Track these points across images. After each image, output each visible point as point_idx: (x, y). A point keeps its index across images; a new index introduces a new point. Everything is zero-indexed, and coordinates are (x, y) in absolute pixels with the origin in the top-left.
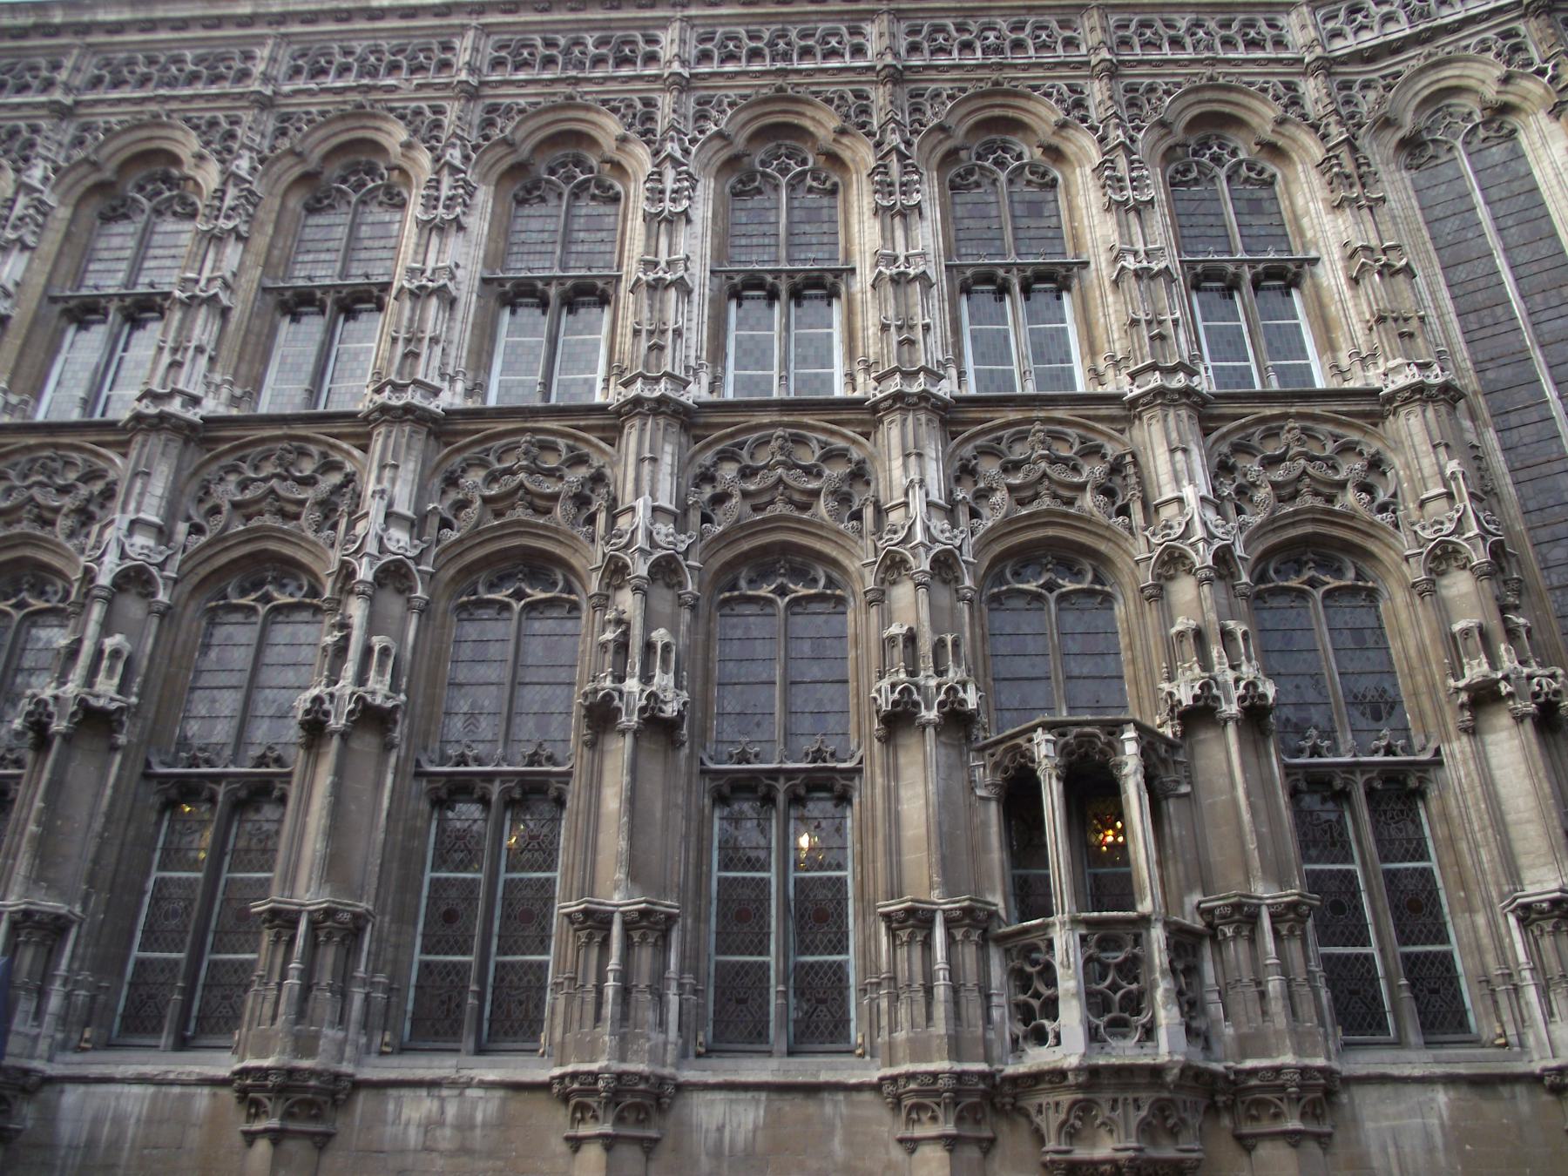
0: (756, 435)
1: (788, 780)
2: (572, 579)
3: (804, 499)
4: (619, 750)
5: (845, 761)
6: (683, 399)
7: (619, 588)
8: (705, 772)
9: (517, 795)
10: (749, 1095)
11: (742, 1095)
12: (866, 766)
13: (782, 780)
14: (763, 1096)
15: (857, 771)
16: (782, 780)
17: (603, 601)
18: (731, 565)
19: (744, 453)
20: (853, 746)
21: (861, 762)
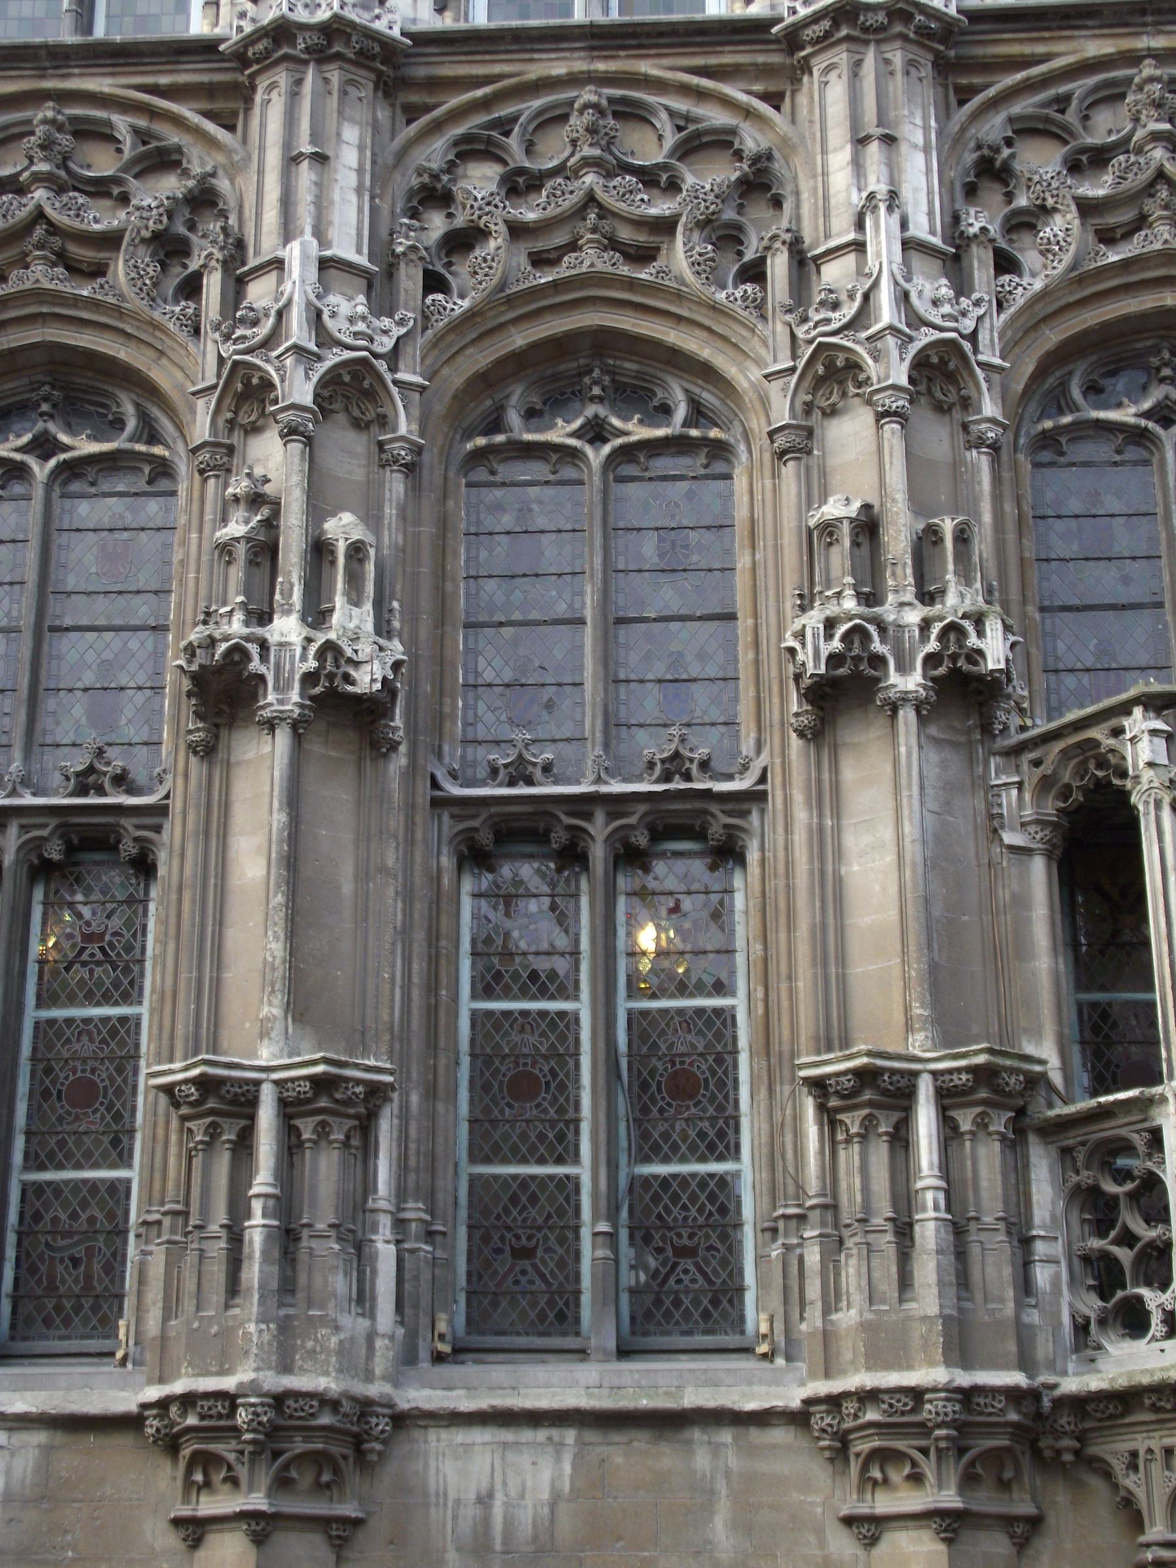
0: (537, 103)
1: (612, 816)
2: (156, 412)
3: (642, 238)
4: (262, 763)
5: (730, 777)
6: (380, 26)
7: (254, 429)
8: (440, 803)
9: (54, 852)
10: (541, 1435)
11: (526, 1435)
12: (774, 786)
13: (600, 817)
14: (570, 1436)
15: (757, 797)
16: (600, 817)
17: (221, 458)
18: (487, 381)
19: (514, 142)
20: (747, 746)
21: (763, 779)
